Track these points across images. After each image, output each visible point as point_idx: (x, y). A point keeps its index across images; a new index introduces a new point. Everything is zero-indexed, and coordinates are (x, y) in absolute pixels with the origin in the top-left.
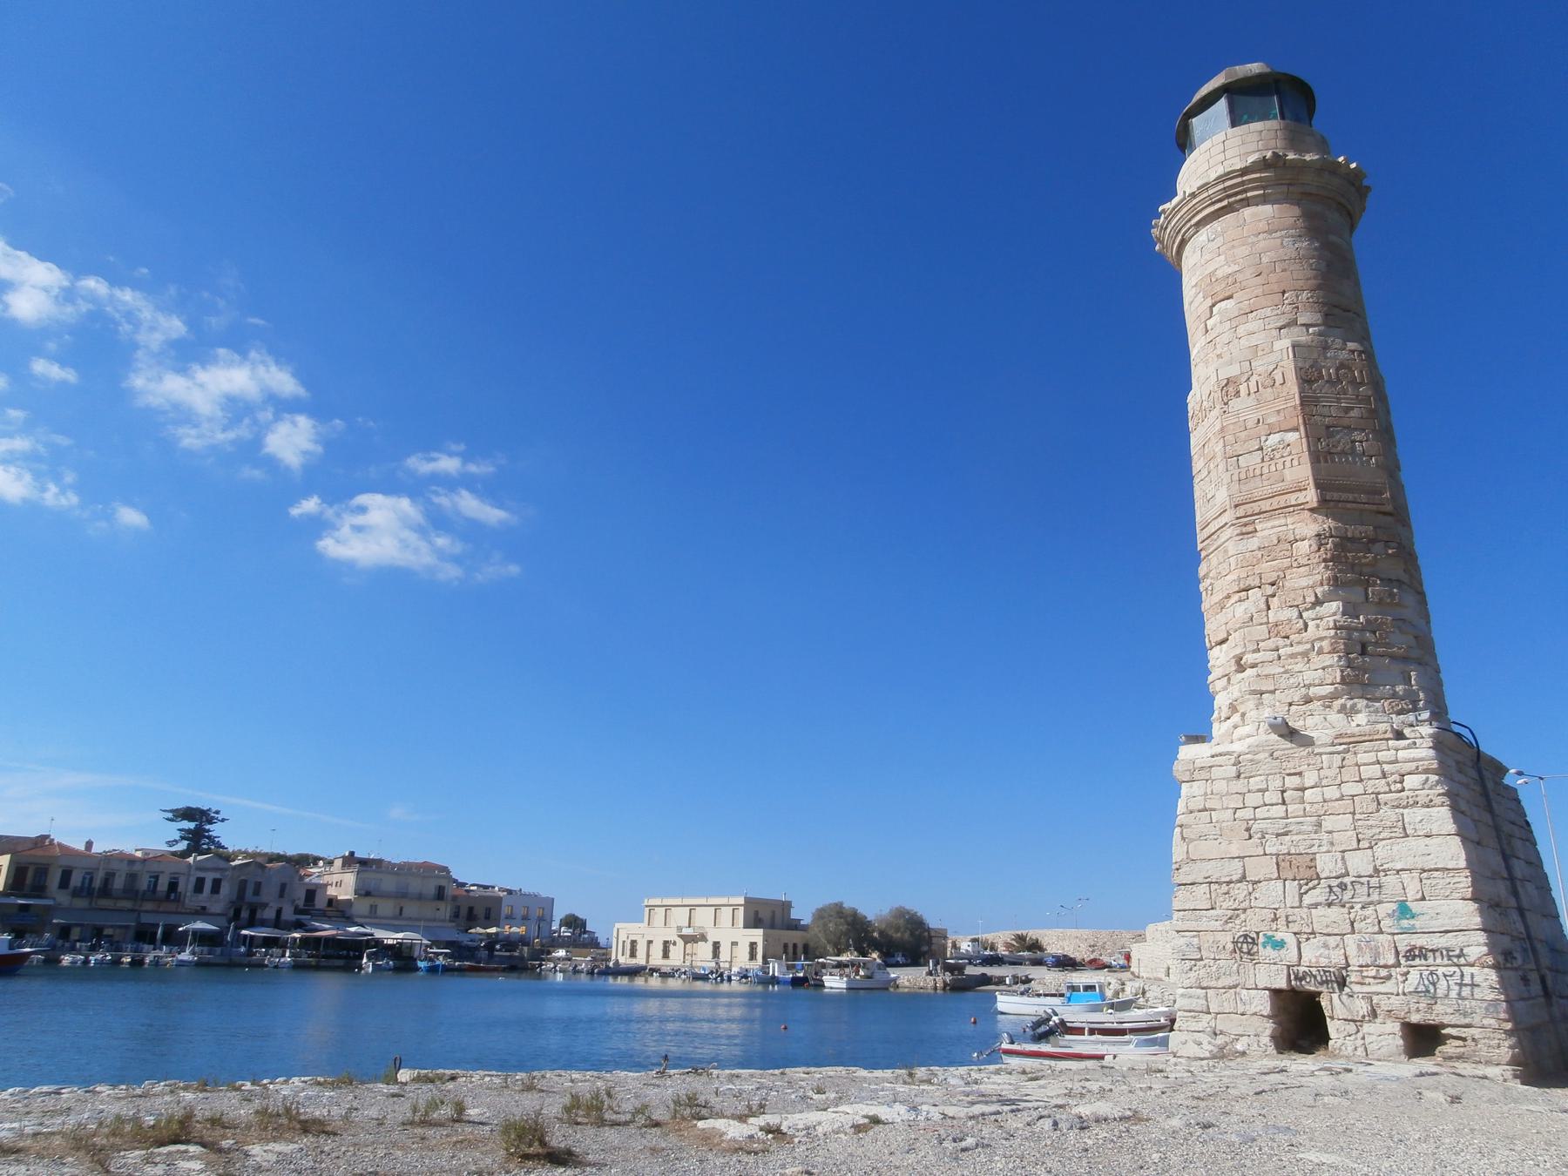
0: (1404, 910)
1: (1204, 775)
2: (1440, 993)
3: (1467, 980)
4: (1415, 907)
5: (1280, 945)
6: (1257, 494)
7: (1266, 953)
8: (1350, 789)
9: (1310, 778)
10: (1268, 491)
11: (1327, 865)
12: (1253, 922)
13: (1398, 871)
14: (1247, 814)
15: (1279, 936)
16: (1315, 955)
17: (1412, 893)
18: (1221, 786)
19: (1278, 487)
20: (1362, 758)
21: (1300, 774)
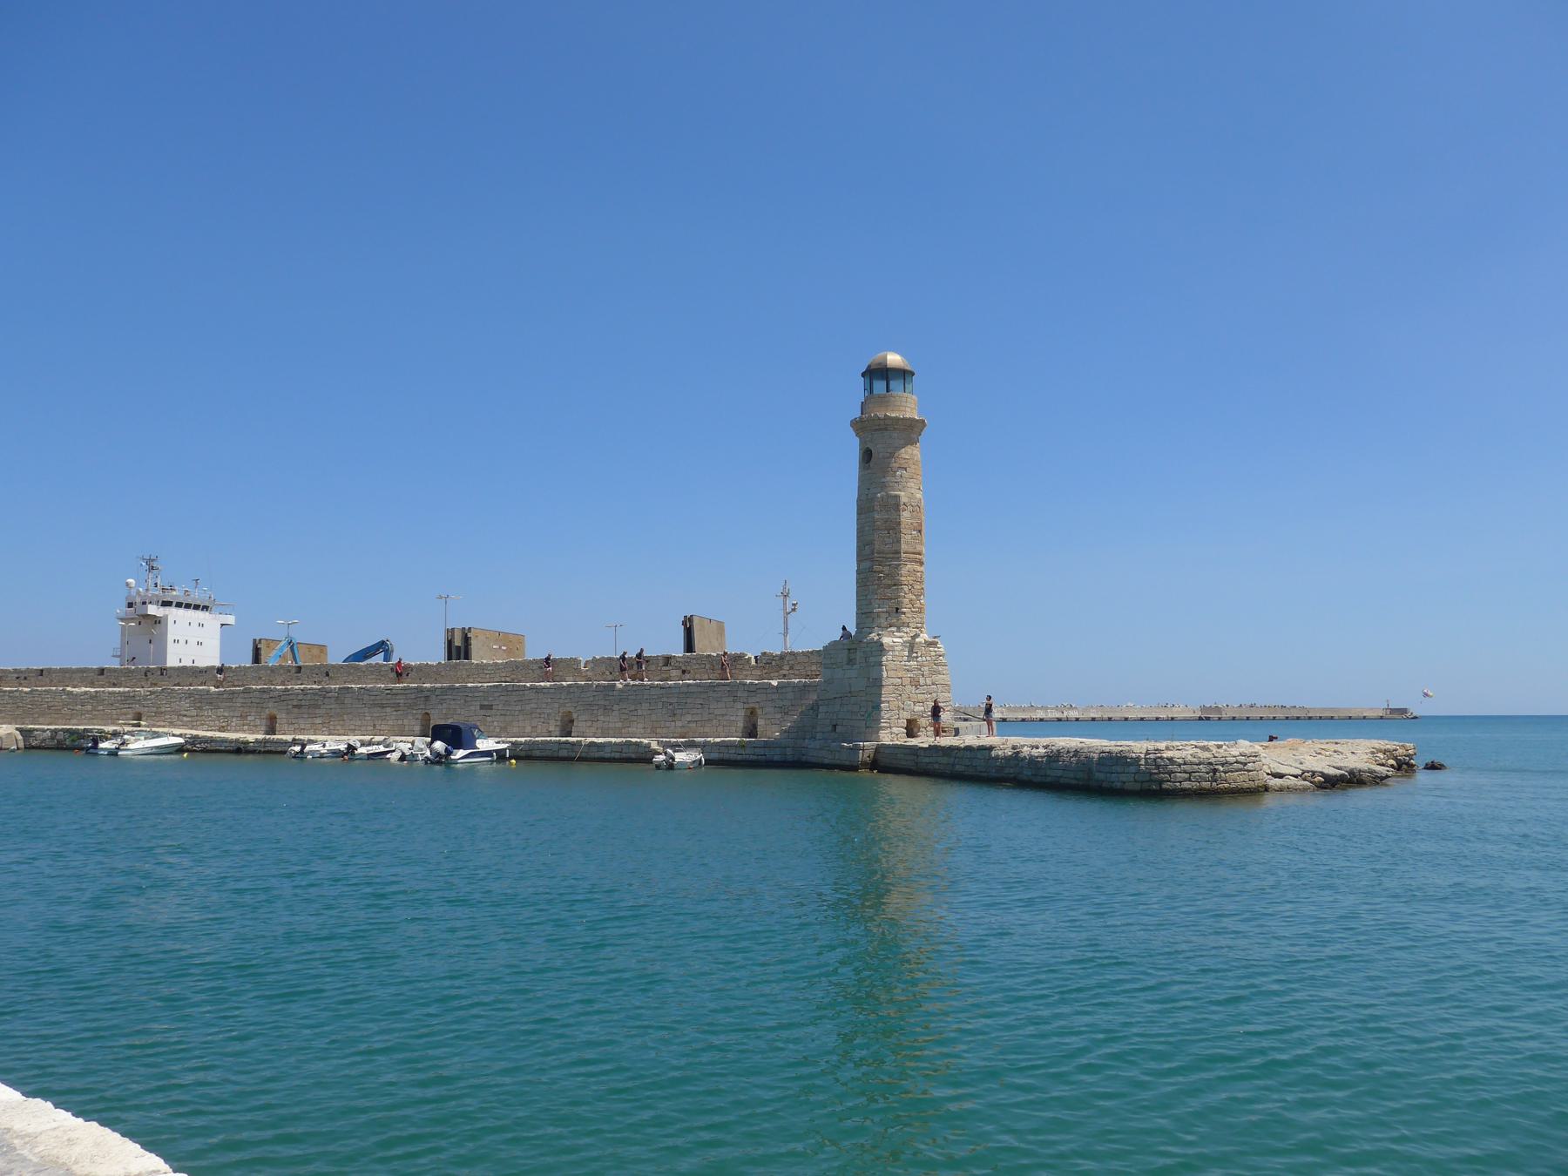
8: (929, 658)
11: (922, 681)
18: (897, 653)
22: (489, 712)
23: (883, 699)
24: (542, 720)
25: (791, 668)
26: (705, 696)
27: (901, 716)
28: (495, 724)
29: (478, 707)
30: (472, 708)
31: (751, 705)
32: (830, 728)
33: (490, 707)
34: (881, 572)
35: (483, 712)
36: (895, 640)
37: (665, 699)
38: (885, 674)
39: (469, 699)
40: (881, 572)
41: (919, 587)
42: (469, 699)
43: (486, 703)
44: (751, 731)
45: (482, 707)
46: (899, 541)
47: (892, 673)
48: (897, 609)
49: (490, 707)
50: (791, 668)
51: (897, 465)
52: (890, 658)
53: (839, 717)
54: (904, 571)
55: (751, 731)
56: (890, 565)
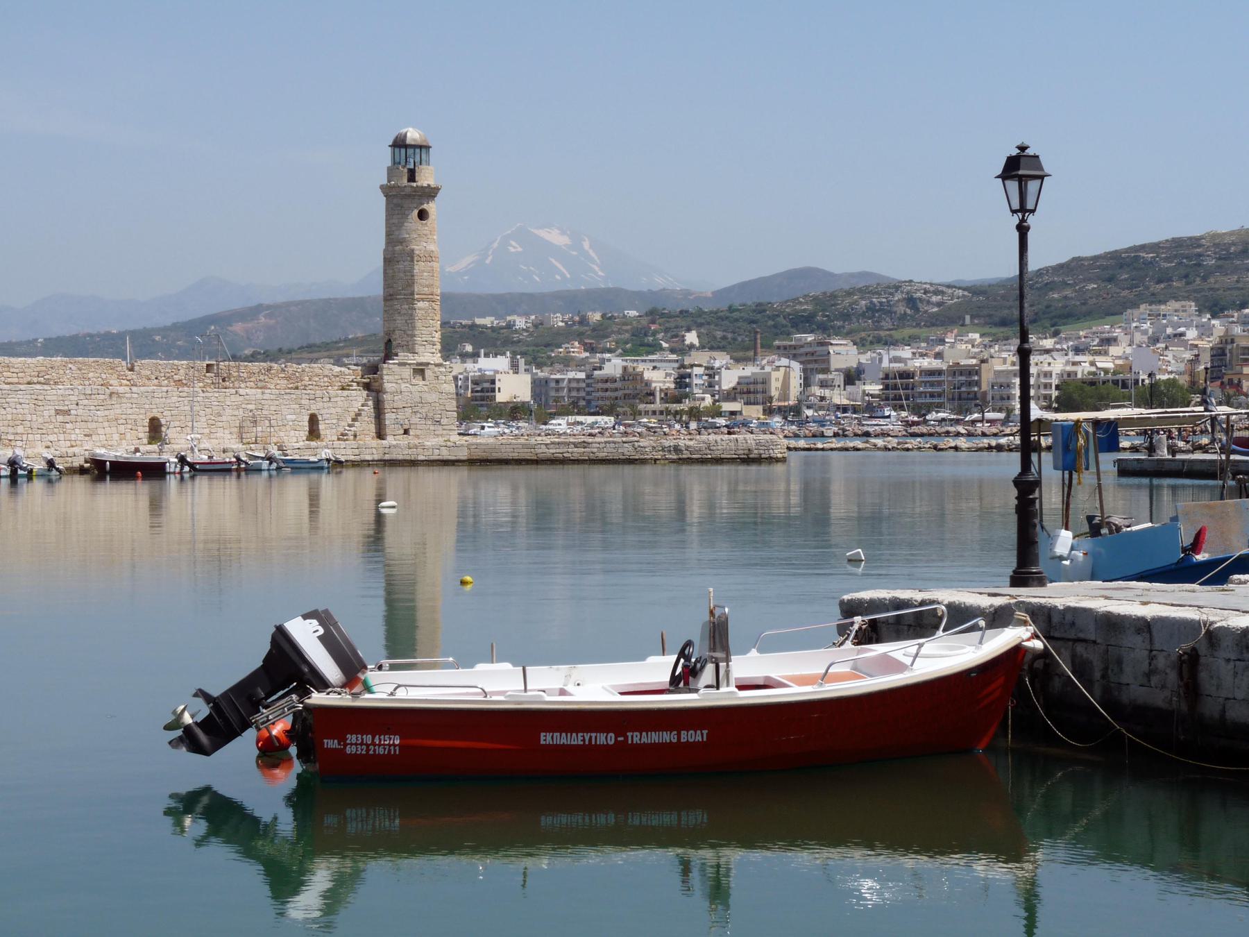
22: (67, 418)
24: (130, 426)
25: (310, 380)
26: (277, 402)
28: (77, 431)
29: (53, 412)
30: (46, 413)
31: (313, 412)
32: (402, 432)
33: (67, 412)
35: (60, 418)
37: (243, 406)
39: (40, 403)
42: (40, 403)
43: (61, 408)
44: (314, 433)
45: (58, 412)
49: (67, 412)
50: (310, 380)
53: (411, 422)
55: (314, 433)
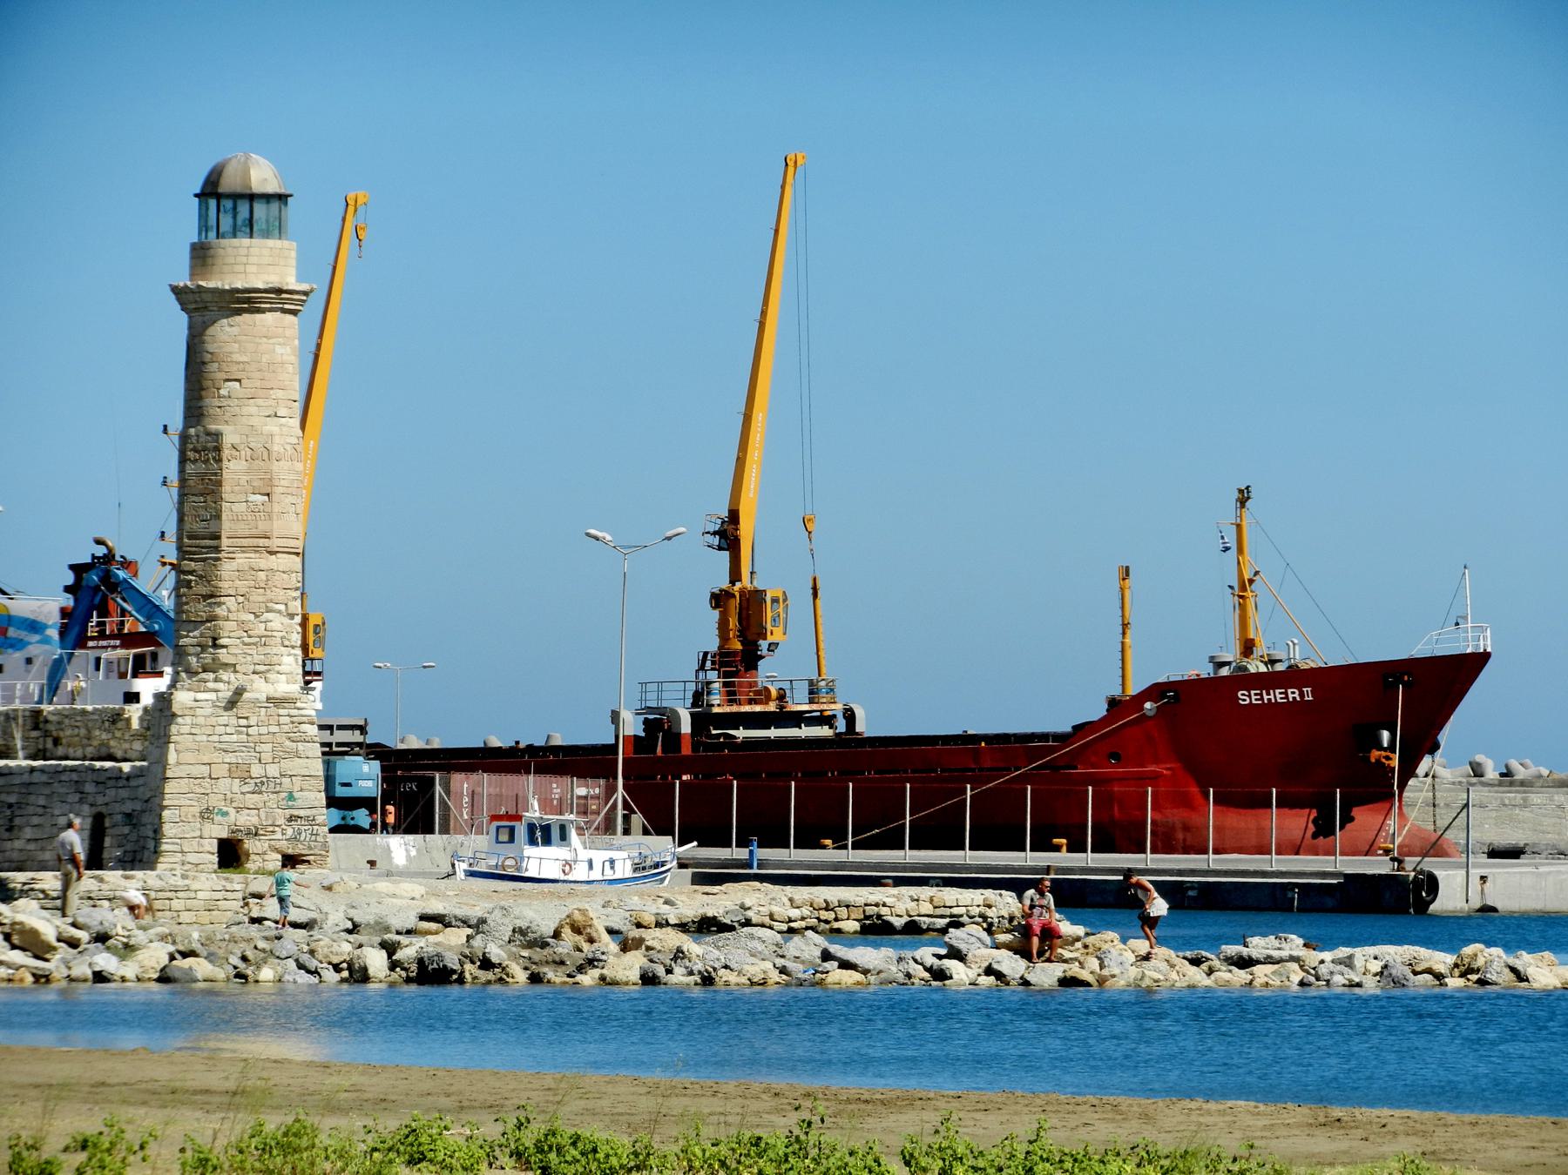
0: (291, 797)
1: (192, 713)
2: (302, 839)
3: (315, 832)
4: (296, 795)
5: (226, 814)
6: (240, 533)
7: (218, 818)
8: (274, 729)
9: (253, 721)
10: (247, 533)
11: (256, 770)
12: (215, 801)
13: (291, 776)
14: (216, 738)
15: (225, 809)
16: (247, 820)
17: (297, 788)
18: (201, 720)
19: (254, 532)
20: (282, 712)
21: (247, 718)
23: (165, 803)
27: (206, 834)
34: (191, 573)
36: (201, 696)
38: (172, 757)
40: (191, 573)
41: (261, 599)
46: (218, 517)
47: (188, 757)
48: (215, 639)
51: (224, 376)
52: (185, 729)
54: (227, 569)
56: (204, 560)
